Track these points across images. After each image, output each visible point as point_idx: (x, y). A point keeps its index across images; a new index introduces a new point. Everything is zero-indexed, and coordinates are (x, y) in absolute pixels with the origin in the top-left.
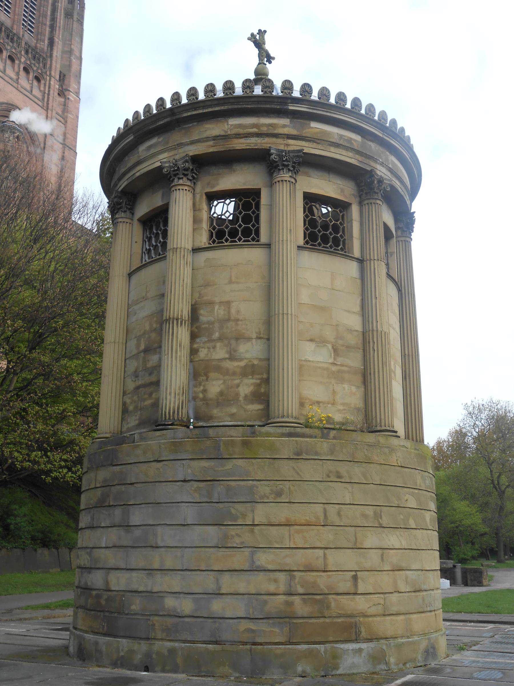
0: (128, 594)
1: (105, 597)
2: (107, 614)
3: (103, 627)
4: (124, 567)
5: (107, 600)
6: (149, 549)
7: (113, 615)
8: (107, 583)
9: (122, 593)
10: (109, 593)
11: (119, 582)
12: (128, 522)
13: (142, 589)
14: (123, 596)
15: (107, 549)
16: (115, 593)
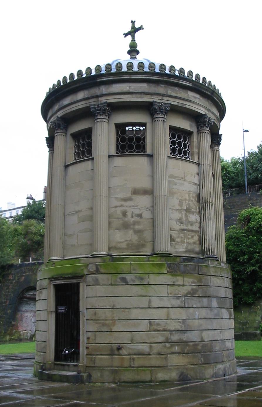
0: (213, 342)
1: (201, 345)
2: (203, 353)
3: (202, 360)
4: (211, 329)
5: (203, 346)
6: (220, 319)
7: (206, 353)
8: (202, 338)
9: (211, 342)
10: (203, 343)
11: (208, 336)
12: (211, 306)
13: (219, 339)
14: (212, 343)
15: (200, 320)
16: (207, 342)
